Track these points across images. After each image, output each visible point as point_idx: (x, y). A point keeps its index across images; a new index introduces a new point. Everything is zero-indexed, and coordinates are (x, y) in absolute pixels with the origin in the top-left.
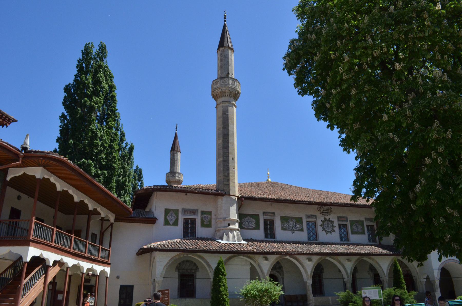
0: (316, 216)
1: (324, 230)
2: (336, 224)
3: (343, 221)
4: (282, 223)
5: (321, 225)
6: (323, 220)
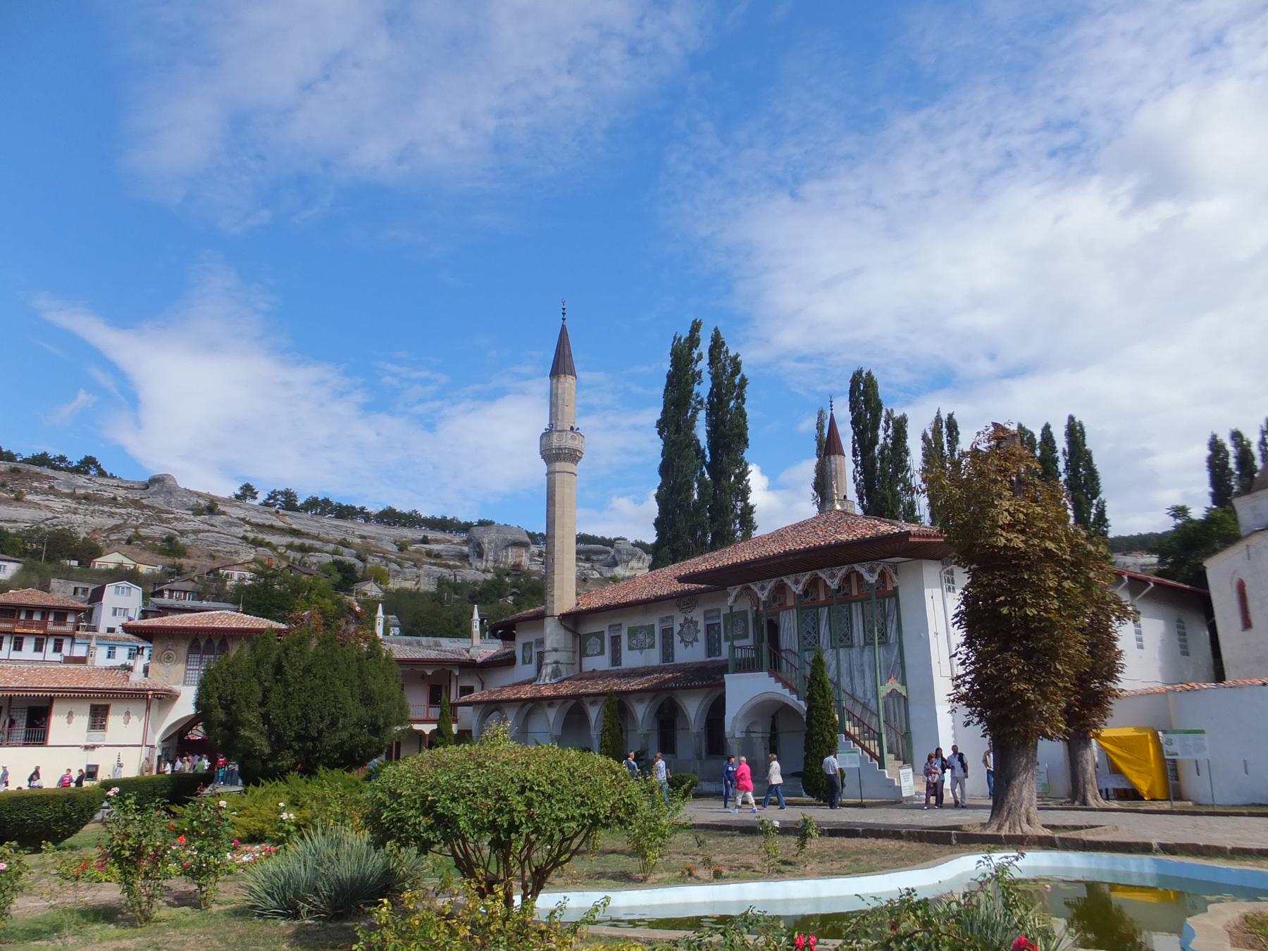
0: (672, 617)
1: (682, 640)
2: (701, 627)
3: (711, 618)
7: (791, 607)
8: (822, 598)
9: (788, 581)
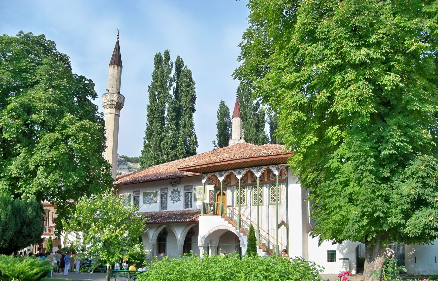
0: (167, 188)
1: (172, 200)
2: (182, 193)
3: (188, 190)
4: (144, 198)
5: (170, 196)
6: (172, 191)
7: (233, 185)
8: (249, 182)
9: (235, 173)
